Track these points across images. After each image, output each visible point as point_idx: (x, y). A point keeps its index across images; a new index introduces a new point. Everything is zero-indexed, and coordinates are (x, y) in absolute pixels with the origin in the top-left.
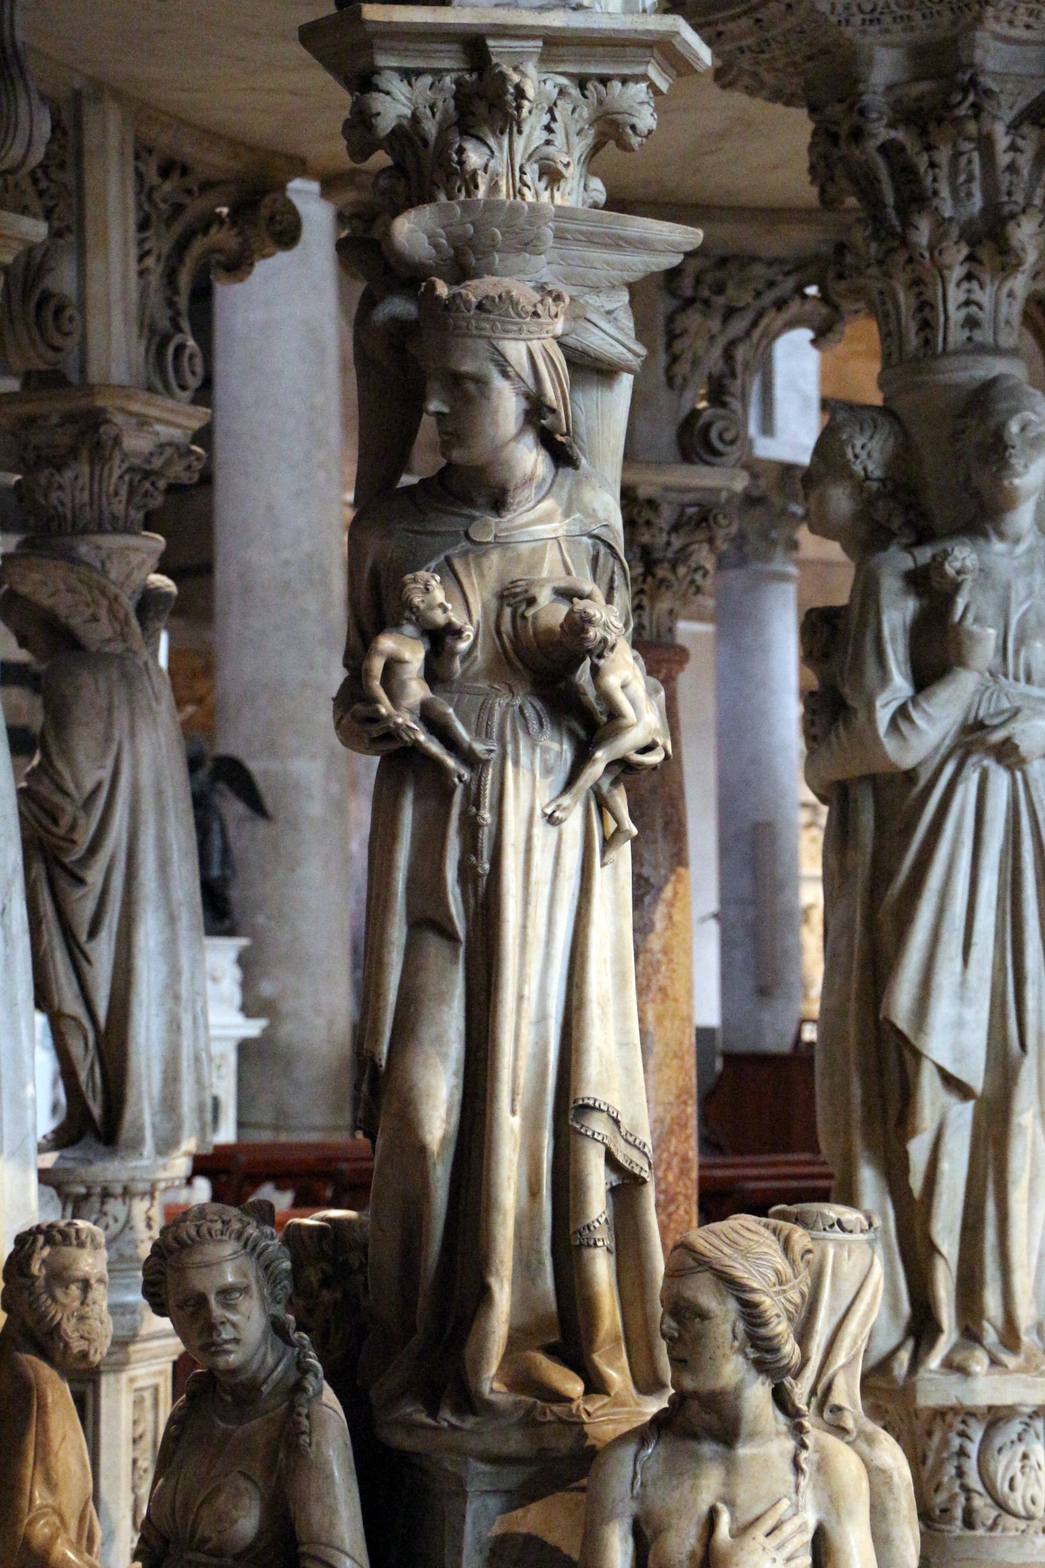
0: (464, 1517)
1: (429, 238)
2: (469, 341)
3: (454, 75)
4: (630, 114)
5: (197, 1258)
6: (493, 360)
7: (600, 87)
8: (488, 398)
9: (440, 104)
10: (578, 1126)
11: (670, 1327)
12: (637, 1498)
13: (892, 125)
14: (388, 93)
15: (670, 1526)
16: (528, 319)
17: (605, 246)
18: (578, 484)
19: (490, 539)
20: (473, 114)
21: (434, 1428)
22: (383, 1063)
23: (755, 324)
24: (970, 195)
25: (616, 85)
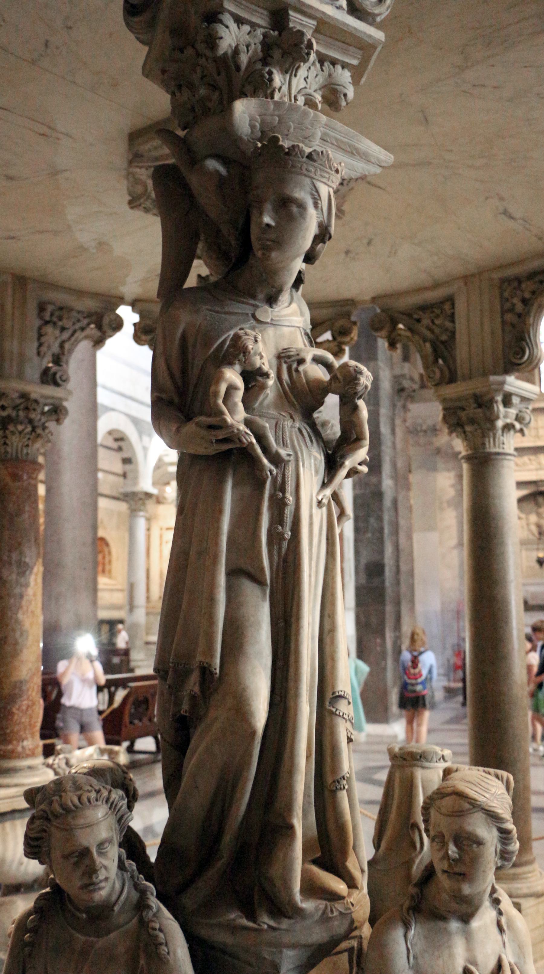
1: (250, 121)
3: (262, 30)
4: (344, 87)
5: (82, 821)
6: (312, 194)
7: (331, 67)
10: (334, 710)
11: (453, 852)
14: (227, 27)
19: (269, 320)
20: (272, 57)
21: (255, 930)
22: (218, 671)
23: (72, 335)
25: (339, 67)
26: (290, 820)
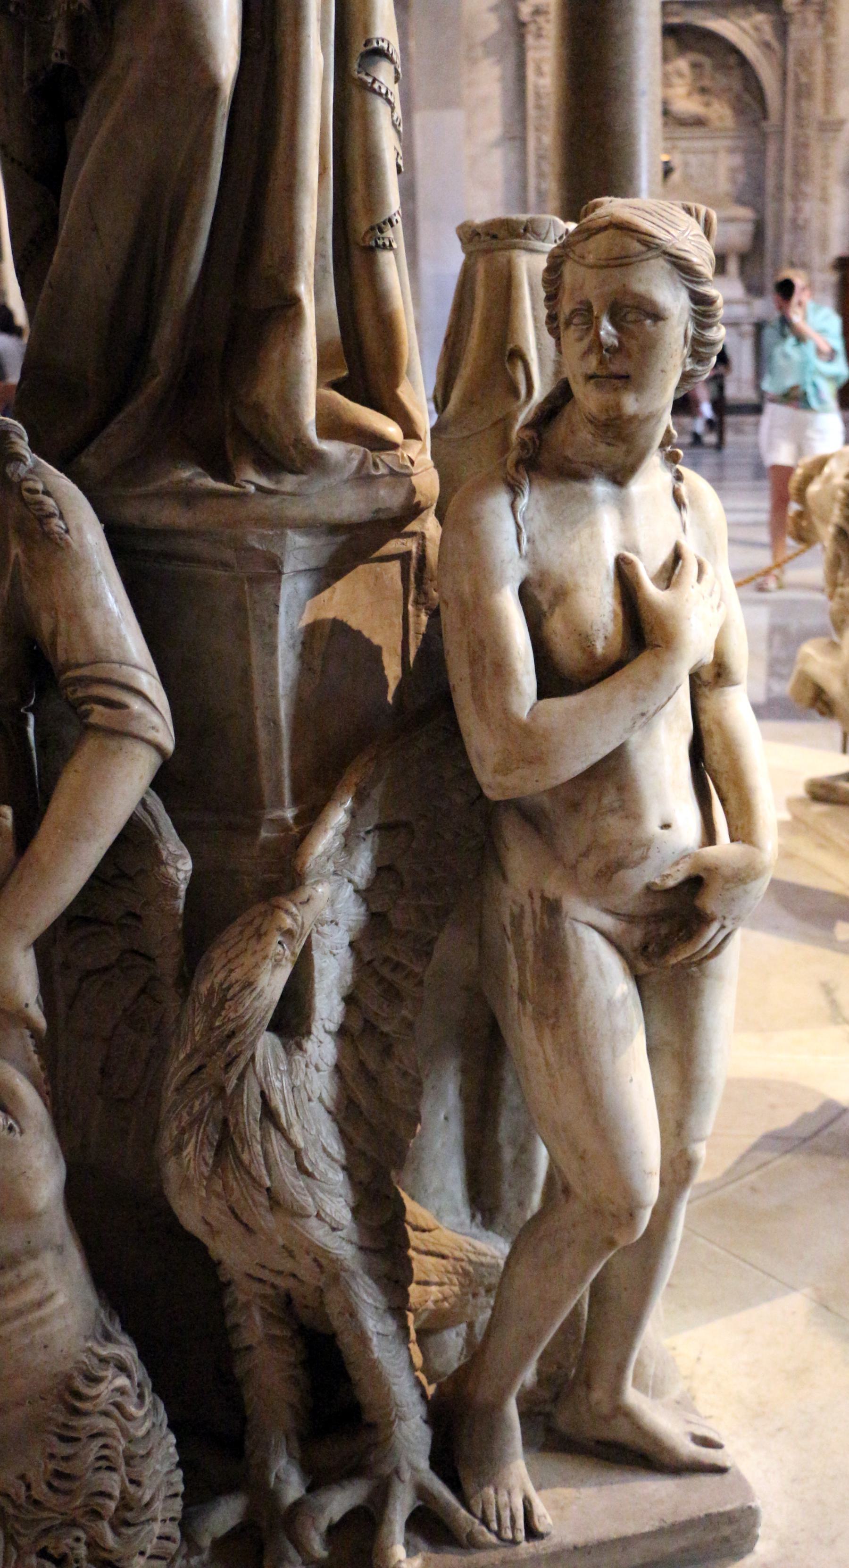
0: (277, 607)
10: (370, 80)
12: (526, 557)
15: (577, 585)
21: (232, 495)
26: (292, 286)
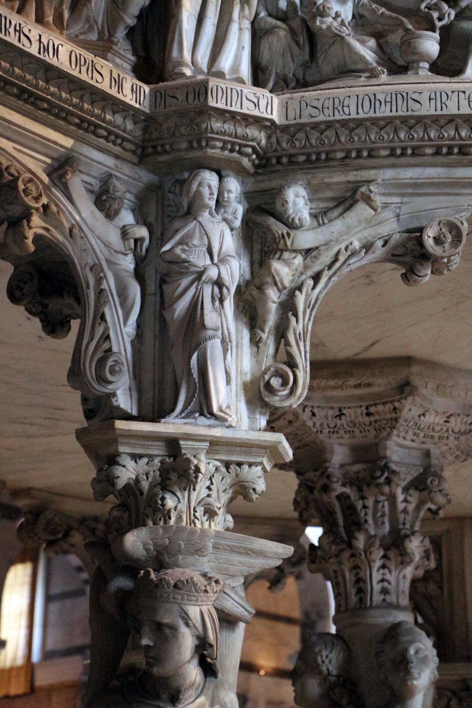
1: (143, 546)
2: (168, 606)
3: (160, 458)
4: (253, 483)
7: (237, 468)
8: (177, 638)
9: (152, 473)
13: (344, 485)
14: (124, 466)
16: (202, 594)
17: (240, 553)
18: (216, 687)
20: (170, 479)
24: (383, 523)
25: (246, 467)
